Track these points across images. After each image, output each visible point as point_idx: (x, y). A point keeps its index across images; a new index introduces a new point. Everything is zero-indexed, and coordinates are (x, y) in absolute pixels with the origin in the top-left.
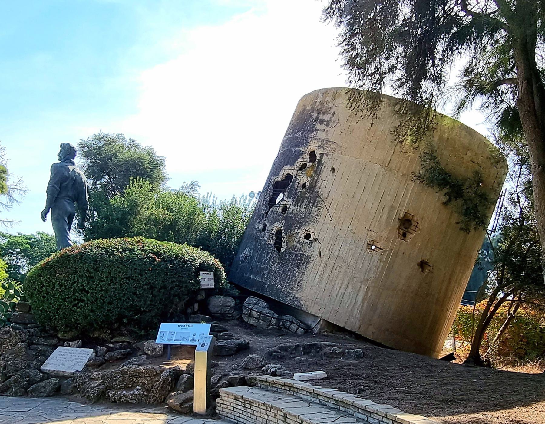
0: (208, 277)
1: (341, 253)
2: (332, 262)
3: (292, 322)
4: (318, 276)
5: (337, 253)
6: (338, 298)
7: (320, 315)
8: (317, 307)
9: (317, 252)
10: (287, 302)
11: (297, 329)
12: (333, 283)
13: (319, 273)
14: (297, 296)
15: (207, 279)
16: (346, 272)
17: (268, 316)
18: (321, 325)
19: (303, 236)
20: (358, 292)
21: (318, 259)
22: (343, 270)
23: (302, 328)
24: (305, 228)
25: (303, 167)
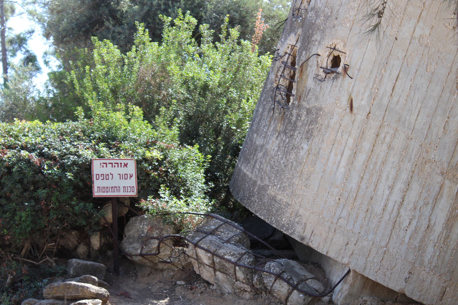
0: (123, 170)
1: (395, 99)
2: (374, 124)
3: (279, 276)
4: (343, 164)
5: (385, 101)
6: (386, 217)
7: (345, 261)
8: (339, 240)
9: (345, 102)
10: (283, 226)
11: (290, 294)
12: (374, 179)
13: (347, 153)
14: (301, 211)
15: (116, 177)
16: (406, 148)
17: (229, 261)
18: (352, 286)
20: (436, 200)
21: (348, 118)
22: (398, 143)
23: (300, 291)
24: (328, 42)
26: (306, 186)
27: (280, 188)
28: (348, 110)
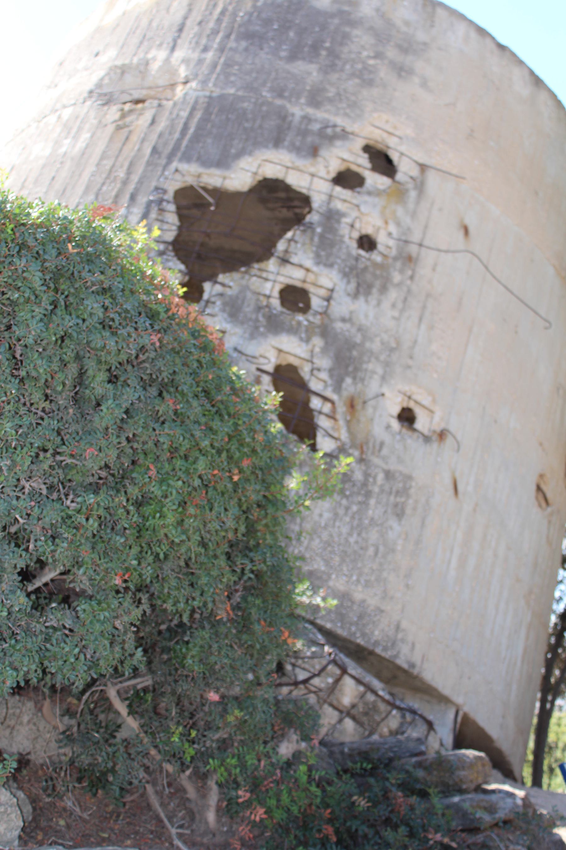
7: (459, 700)
10: (377, 643)
14: (404, 624)
19: (396, 410)
25: (347, 179)
26: (407, 586)
27: (358, 581)
28: (452, 491)
